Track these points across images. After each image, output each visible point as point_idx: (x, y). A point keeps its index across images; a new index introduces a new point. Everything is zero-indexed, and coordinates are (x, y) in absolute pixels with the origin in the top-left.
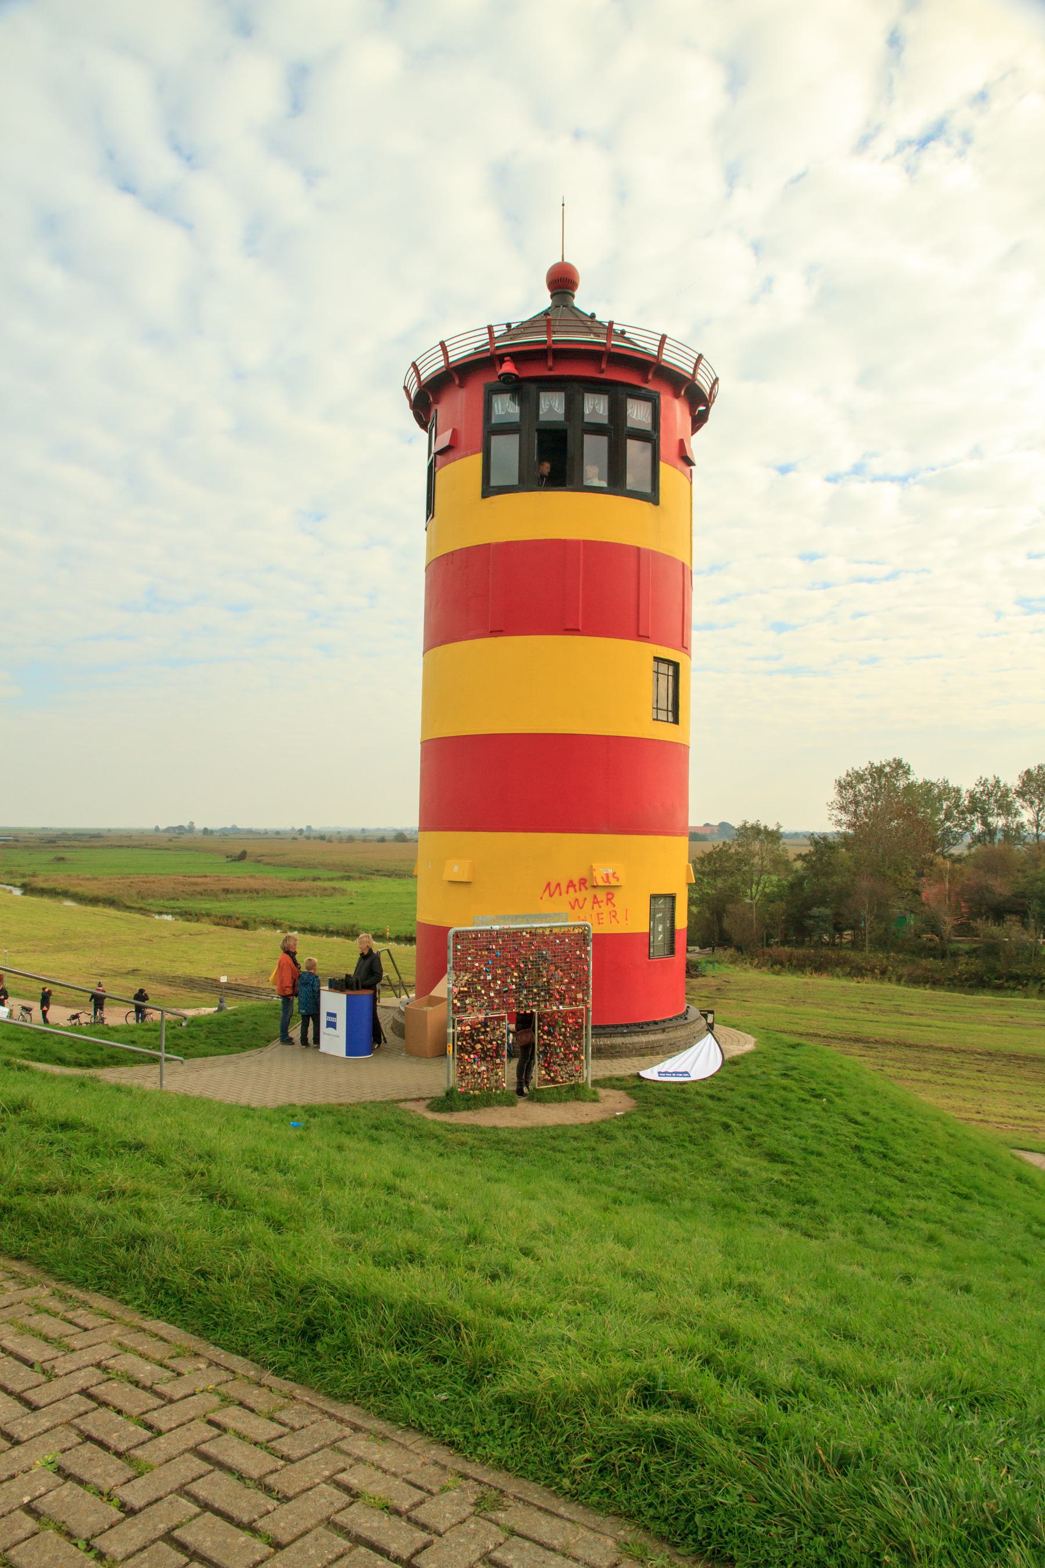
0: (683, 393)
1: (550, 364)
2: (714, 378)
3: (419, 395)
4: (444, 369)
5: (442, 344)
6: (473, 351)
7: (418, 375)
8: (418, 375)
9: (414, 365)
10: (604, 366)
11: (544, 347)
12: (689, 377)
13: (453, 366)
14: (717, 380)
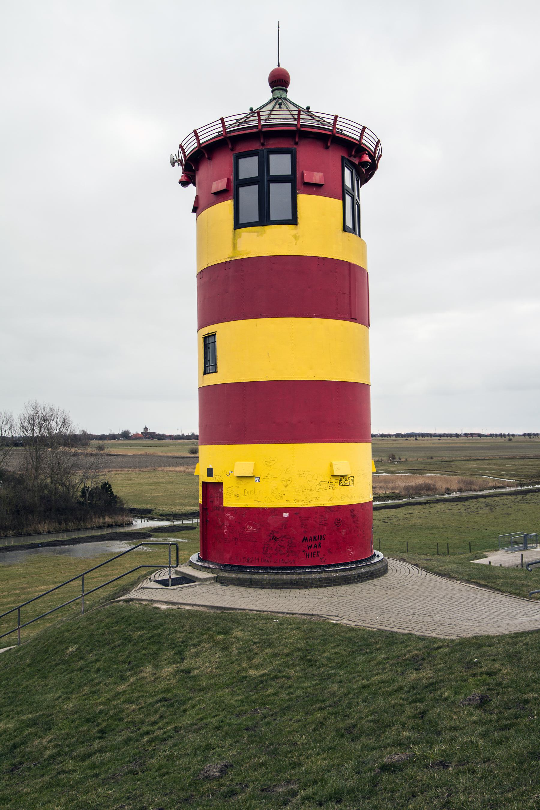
0: (353, 153)
2: (377, 140)
4: (197, 149)
5: (195, 132)
13: (203, 145)
14: (379, 142)
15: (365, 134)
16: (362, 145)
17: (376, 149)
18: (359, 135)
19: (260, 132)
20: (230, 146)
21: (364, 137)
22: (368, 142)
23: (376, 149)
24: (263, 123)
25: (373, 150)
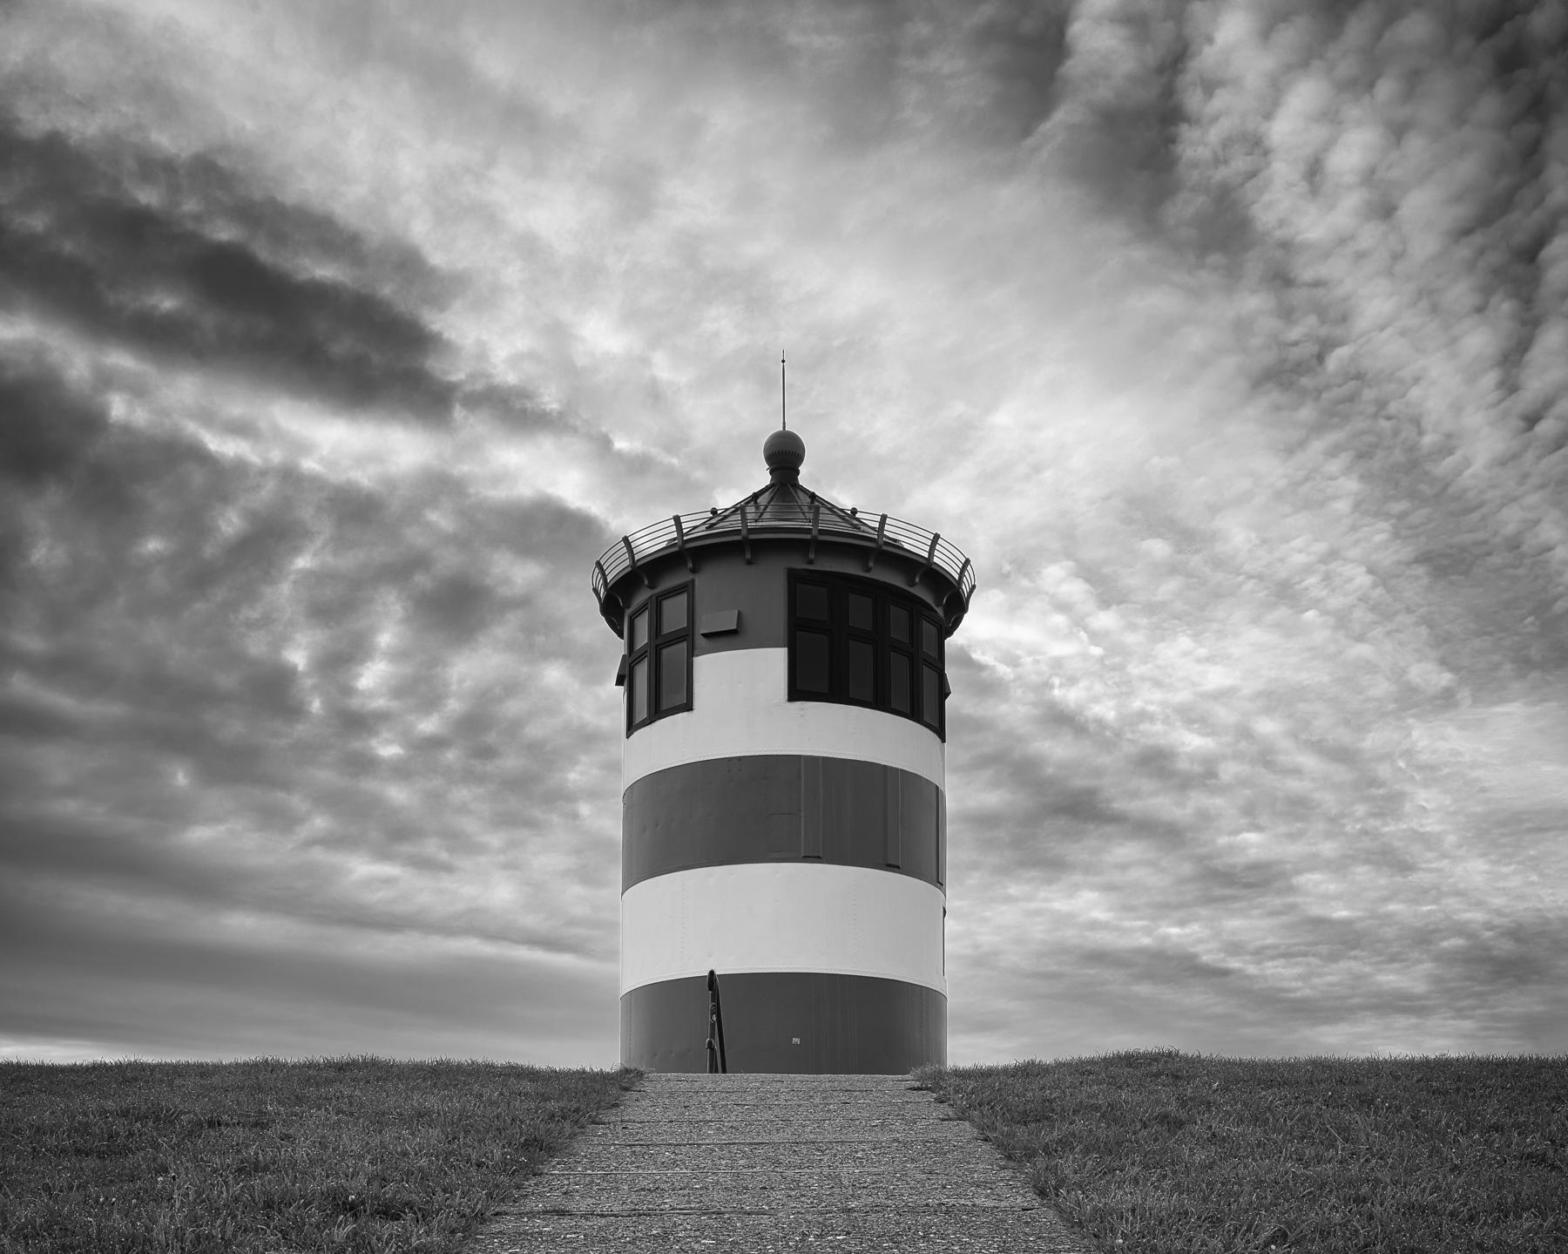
0: (917, 580)
1: (748, 556)
2: (963, 560)
3: (607, 597)
4: (630, 569)
6: (664, 545)
7: (604, 576)
8: (604, 576)
9: (598, 564)
10: (812, 556)
11: (738, 538)
12: (924, 561)
13: (639, 563)
14: (967, 562)
15: (938, 547)
16: (933, 566)
17: (961, 574)
18: (928, 549)
19: (745, 539)
20: (690, 565)
21: (936, 553)
22: (946, 561)
23: (961, 574)
24: (751, 525)
25: (957, 577)
